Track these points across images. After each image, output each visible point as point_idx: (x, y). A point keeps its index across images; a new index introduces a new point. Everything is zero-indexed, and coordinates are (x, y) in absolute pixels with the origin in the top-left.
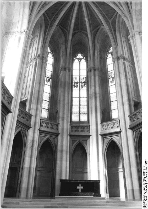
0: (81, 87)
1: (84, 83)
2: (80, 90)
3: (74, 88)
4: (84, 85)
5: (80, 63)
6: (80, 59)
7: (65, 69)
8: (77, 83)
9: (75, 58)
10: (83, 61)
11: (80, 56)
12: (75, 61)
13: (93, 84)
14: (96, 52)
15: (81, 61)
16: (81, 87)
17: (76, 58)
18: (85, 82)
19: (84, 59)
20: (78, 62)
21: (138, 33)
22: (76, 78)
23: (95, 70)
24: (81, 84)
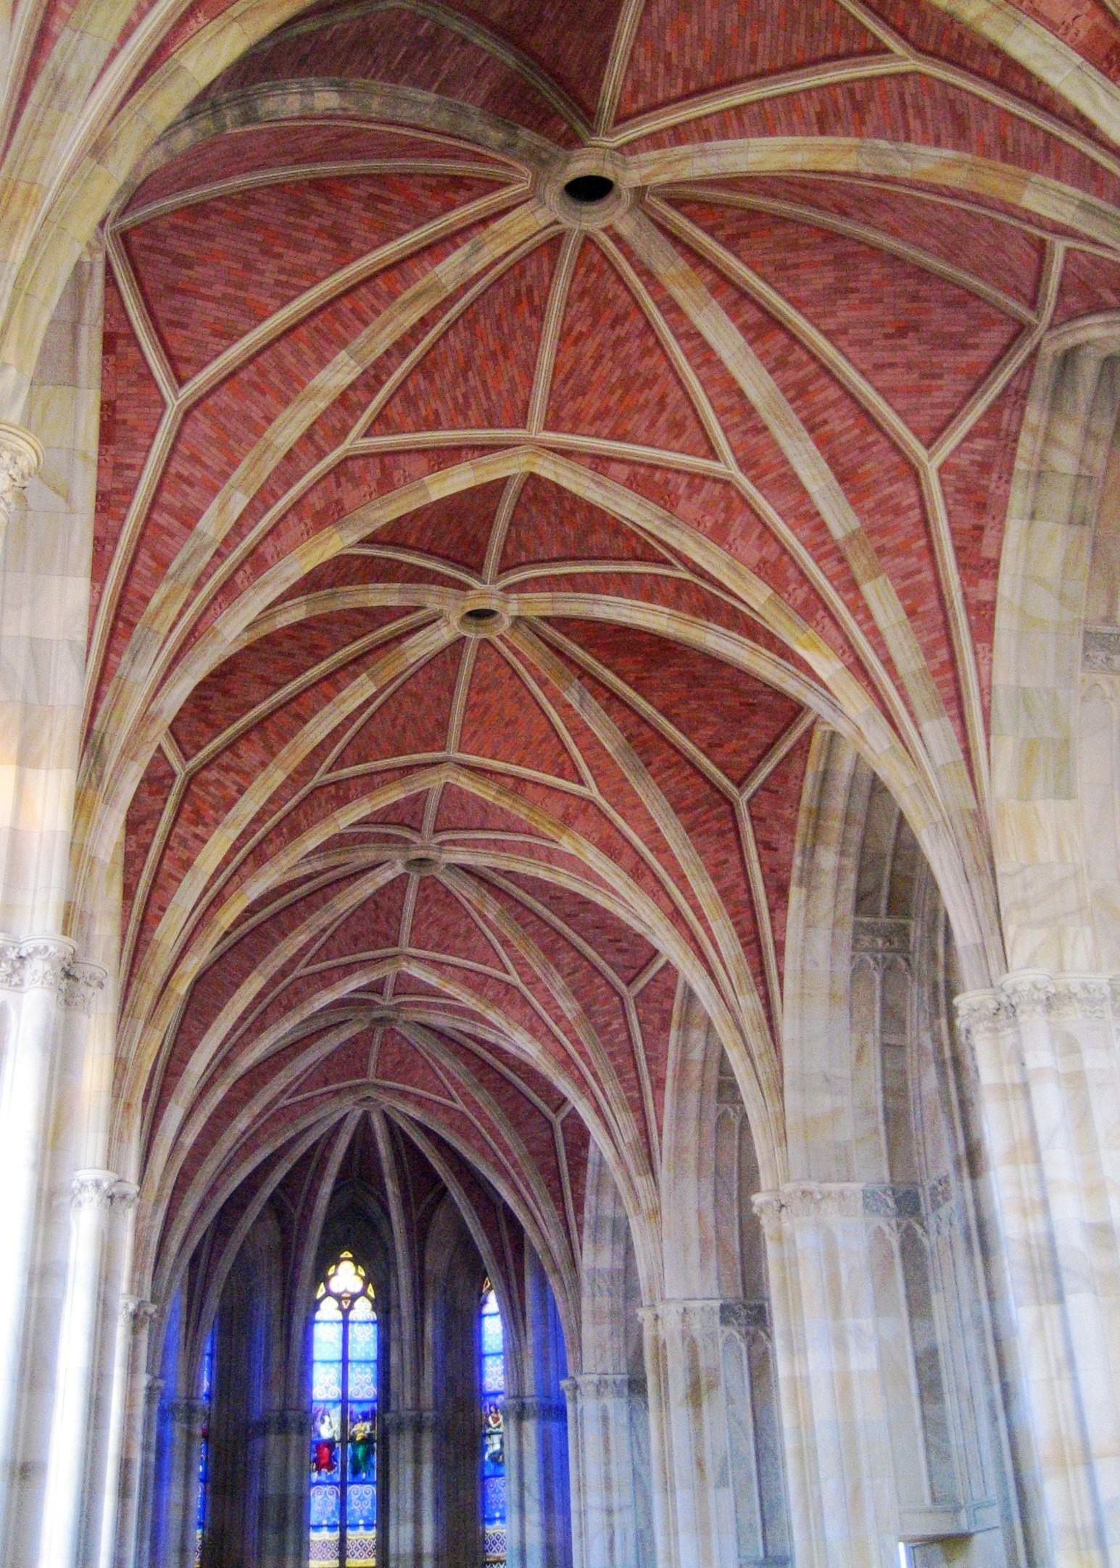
0: (349, 1470)
1: (367, 1440)
2: (343, 1485)
3: (315, 1476)
4: (368, 1454)
5: (345, 1323)
6: (346, 1302)
7: (283, 1426)
8: (330, 1444)
9: (321, 1291)
10: (363, 1309)
11: (346, 1276)
12: (323, 1305)
13: (409, 1505)
14: (429, 1321)
15: (351, 1308)
16: (349, 1470)
17: (328, 1293)
18: (369, 1435)
19: (368, 1297)
20: (339, 1316)
21: (591, 1388)
22: (327, 1418)
23: (418, 1428)
24: (349, 1446)
